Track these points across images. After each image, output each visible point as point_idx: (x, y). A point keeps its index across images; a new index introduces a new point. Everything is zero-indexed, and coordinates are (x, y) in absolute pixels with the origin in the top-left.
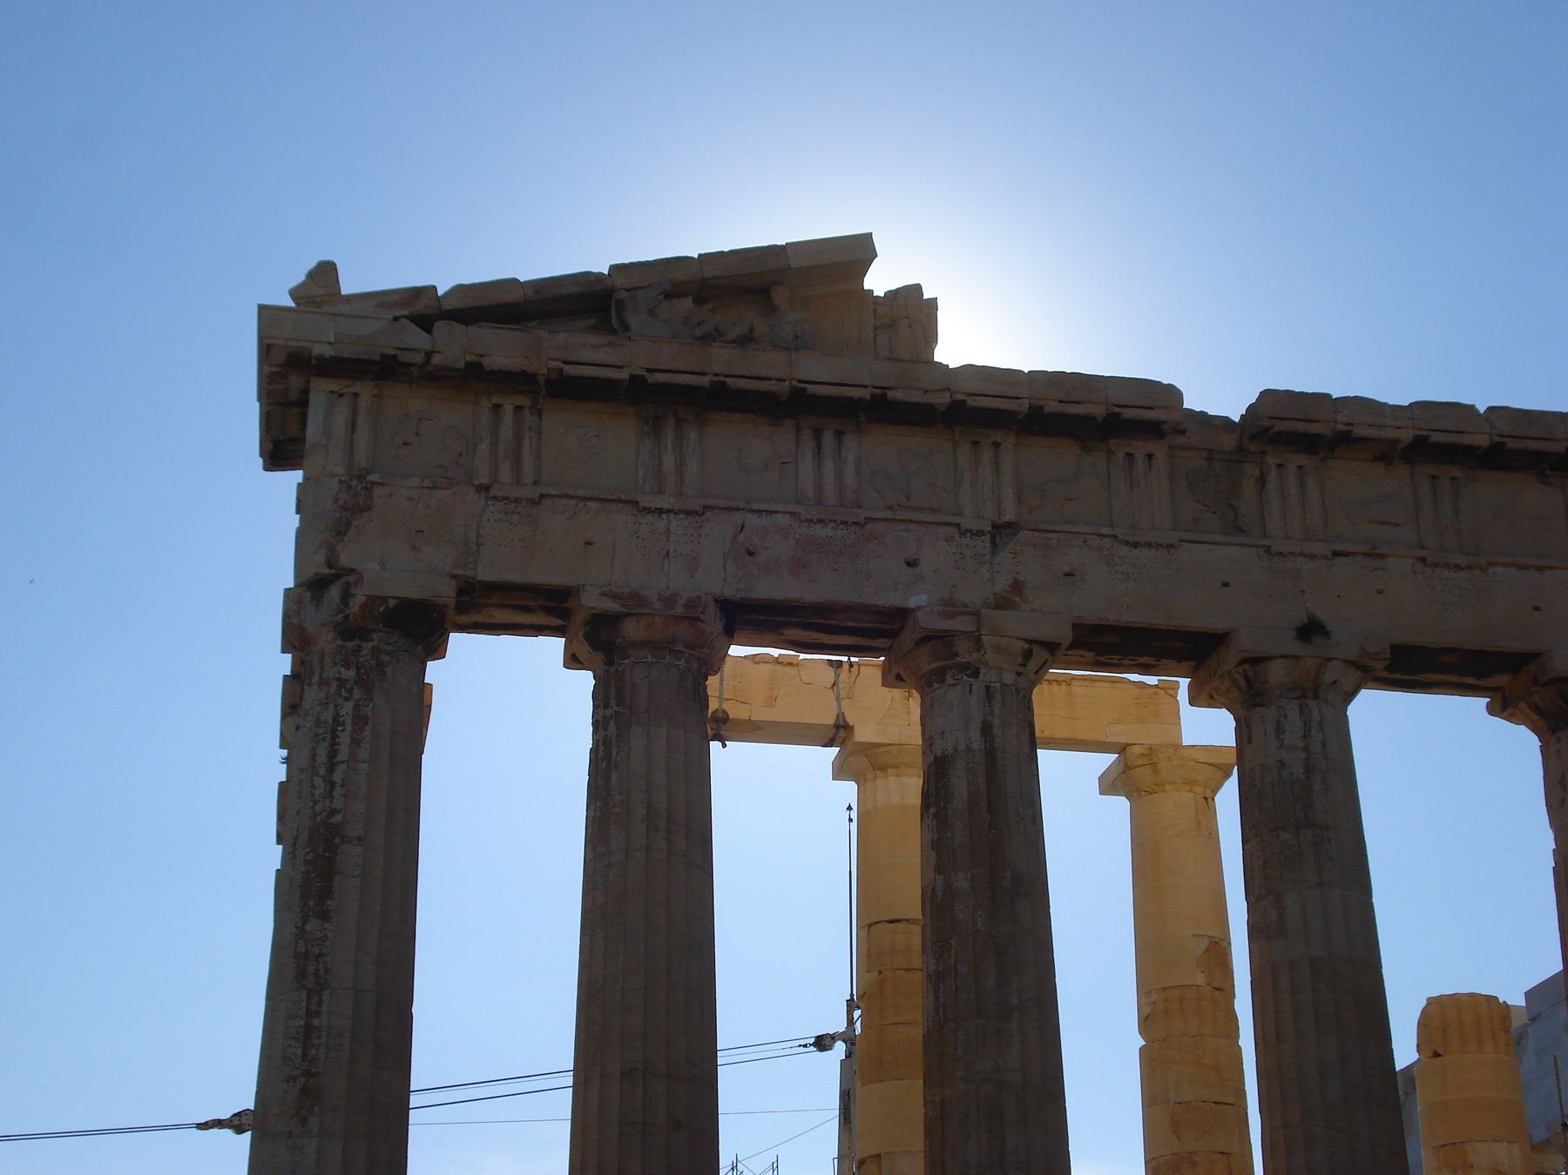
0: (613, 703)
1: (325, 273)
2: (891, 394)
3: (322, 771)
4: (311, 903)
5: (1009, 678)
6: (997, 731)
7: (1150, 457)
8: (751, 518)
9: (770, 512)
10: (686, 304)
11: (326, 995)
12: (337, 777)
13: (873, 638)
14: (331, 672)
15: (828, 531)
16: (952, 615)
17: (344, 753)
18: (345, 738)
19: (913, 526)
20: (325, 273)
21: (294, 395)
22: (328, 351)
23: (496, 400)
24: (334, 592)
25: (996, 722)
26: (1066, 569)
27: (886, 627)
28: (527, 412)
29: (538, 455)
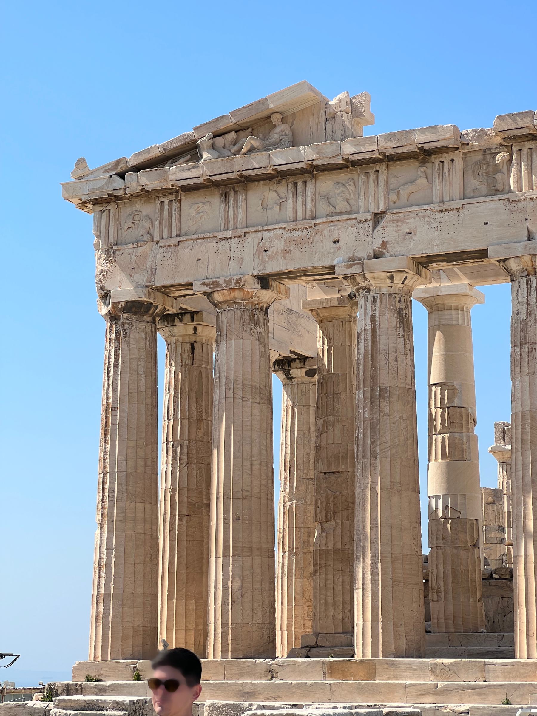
1: (81, 161)
2: (314, 163)
5: (384, 290)
6: (377, 319)
7: (452, 160)
8: (266, 234)
10: (233, 134)
15: (299, 233)
16: (351, 266)
18: (112, 365)
19: (337, 223)
20: (81, 161)
23: (161, 199)
25: (377, 314)
26: (408, 231)
28: (174, 202)
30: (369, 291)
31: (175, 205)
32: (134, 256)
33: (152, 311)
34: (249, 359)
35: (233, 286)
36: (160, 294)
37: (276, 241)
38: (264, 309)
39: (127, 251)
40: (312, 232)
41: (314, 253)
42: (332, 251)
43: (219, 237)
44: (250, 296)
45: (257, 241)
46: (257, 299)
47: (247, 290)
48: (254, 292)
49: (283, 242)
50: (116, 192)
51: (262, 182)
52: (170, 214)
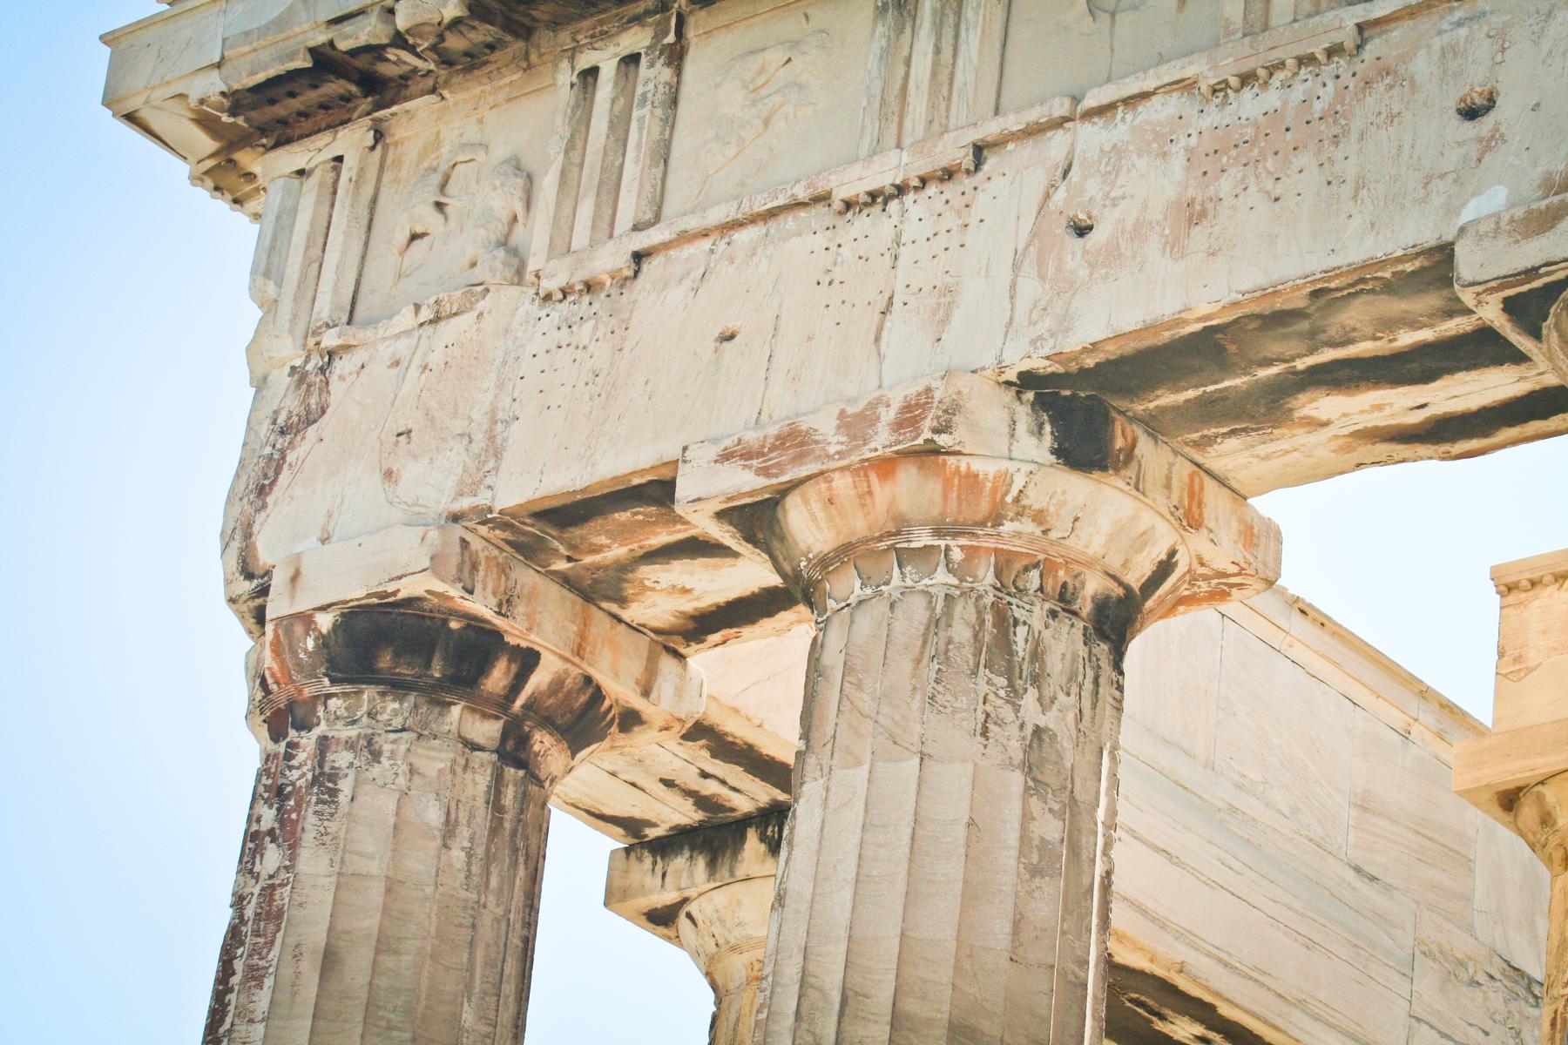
9: (1132, 101)
15: (1271, 98)
23: (585, 60)
28: (644, 61)
29: (663, 154)
31: (654, 75)
32: (414, 372)
33: (498, 678)
34: (951, 870)
35: (882, 441)
36: (554, 591)
37: (1142, 163)
38: (1086, 607)
39: (386, 351)
40: (1346, 78)
41: (1346, 191)
42: (1452, 160)
43: (841, 194)
44: (984, 507)
45: (1038, 179)
46: (1028, 526)
47: (963, 463)
48: (1005, 480)
49: (1178, 163)
50: (347, 28)
52: (620, 127)
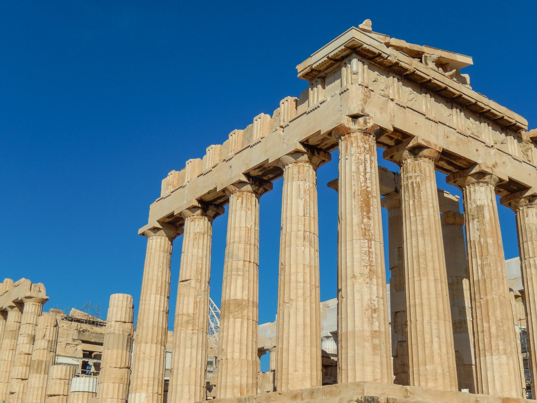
0: (419, 172)
2: (478, 103)
3: (362, 174)
4: (365, 214)
6: (494, 202)
11: (373, 242)
12: (368, 175)
13: (456, 169)
14: (361, 144)
15: (462, 136)
16: (488, 167)
17: (368, 170)
21: (337, 58)
22: (368, 47)
24: (361, 120)
27: (464, 166)
30: (488, 185)
35: (438, 150)
51: (440, 98)
